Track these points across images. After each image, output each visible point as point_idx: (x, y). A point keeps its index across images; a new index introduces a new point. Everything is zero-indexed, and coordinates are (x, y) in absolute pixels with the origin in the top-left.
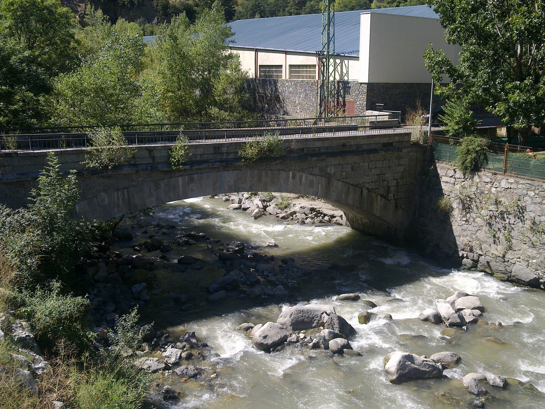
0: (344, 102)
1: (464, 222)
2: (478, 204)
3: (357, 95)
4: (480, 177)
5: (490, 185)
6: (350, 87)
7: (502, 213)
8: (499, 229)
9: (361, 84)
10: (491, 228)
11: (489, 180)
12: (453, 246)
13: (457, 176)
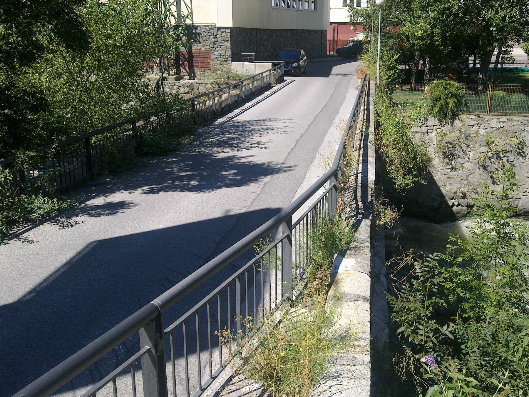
0: (190, 53)
1: (449, 170)
2: (464, 148)
3: (214, 43)
4: (461, 120)
5: (478, 128)
6: (199, 34)
7: (497, 153)
8: (497, 169)
9: (220, 28)
10: (487, 170)
11: (476, 123)
12: (437, 197)
13: (430, 123)
